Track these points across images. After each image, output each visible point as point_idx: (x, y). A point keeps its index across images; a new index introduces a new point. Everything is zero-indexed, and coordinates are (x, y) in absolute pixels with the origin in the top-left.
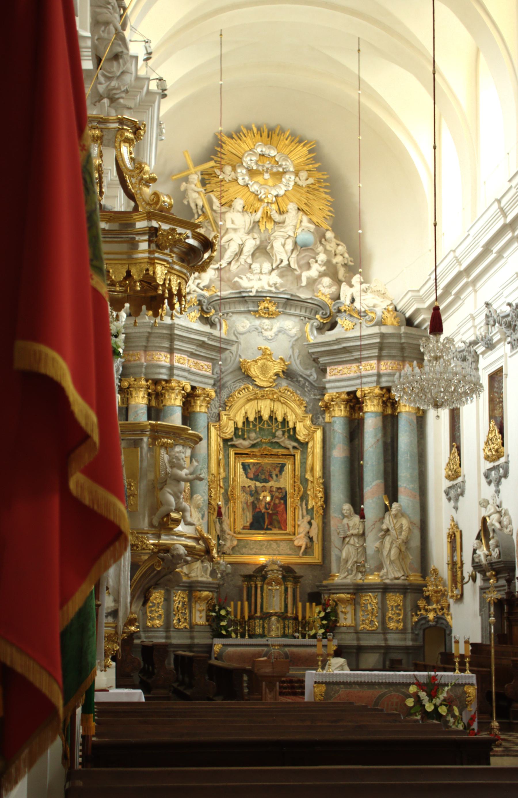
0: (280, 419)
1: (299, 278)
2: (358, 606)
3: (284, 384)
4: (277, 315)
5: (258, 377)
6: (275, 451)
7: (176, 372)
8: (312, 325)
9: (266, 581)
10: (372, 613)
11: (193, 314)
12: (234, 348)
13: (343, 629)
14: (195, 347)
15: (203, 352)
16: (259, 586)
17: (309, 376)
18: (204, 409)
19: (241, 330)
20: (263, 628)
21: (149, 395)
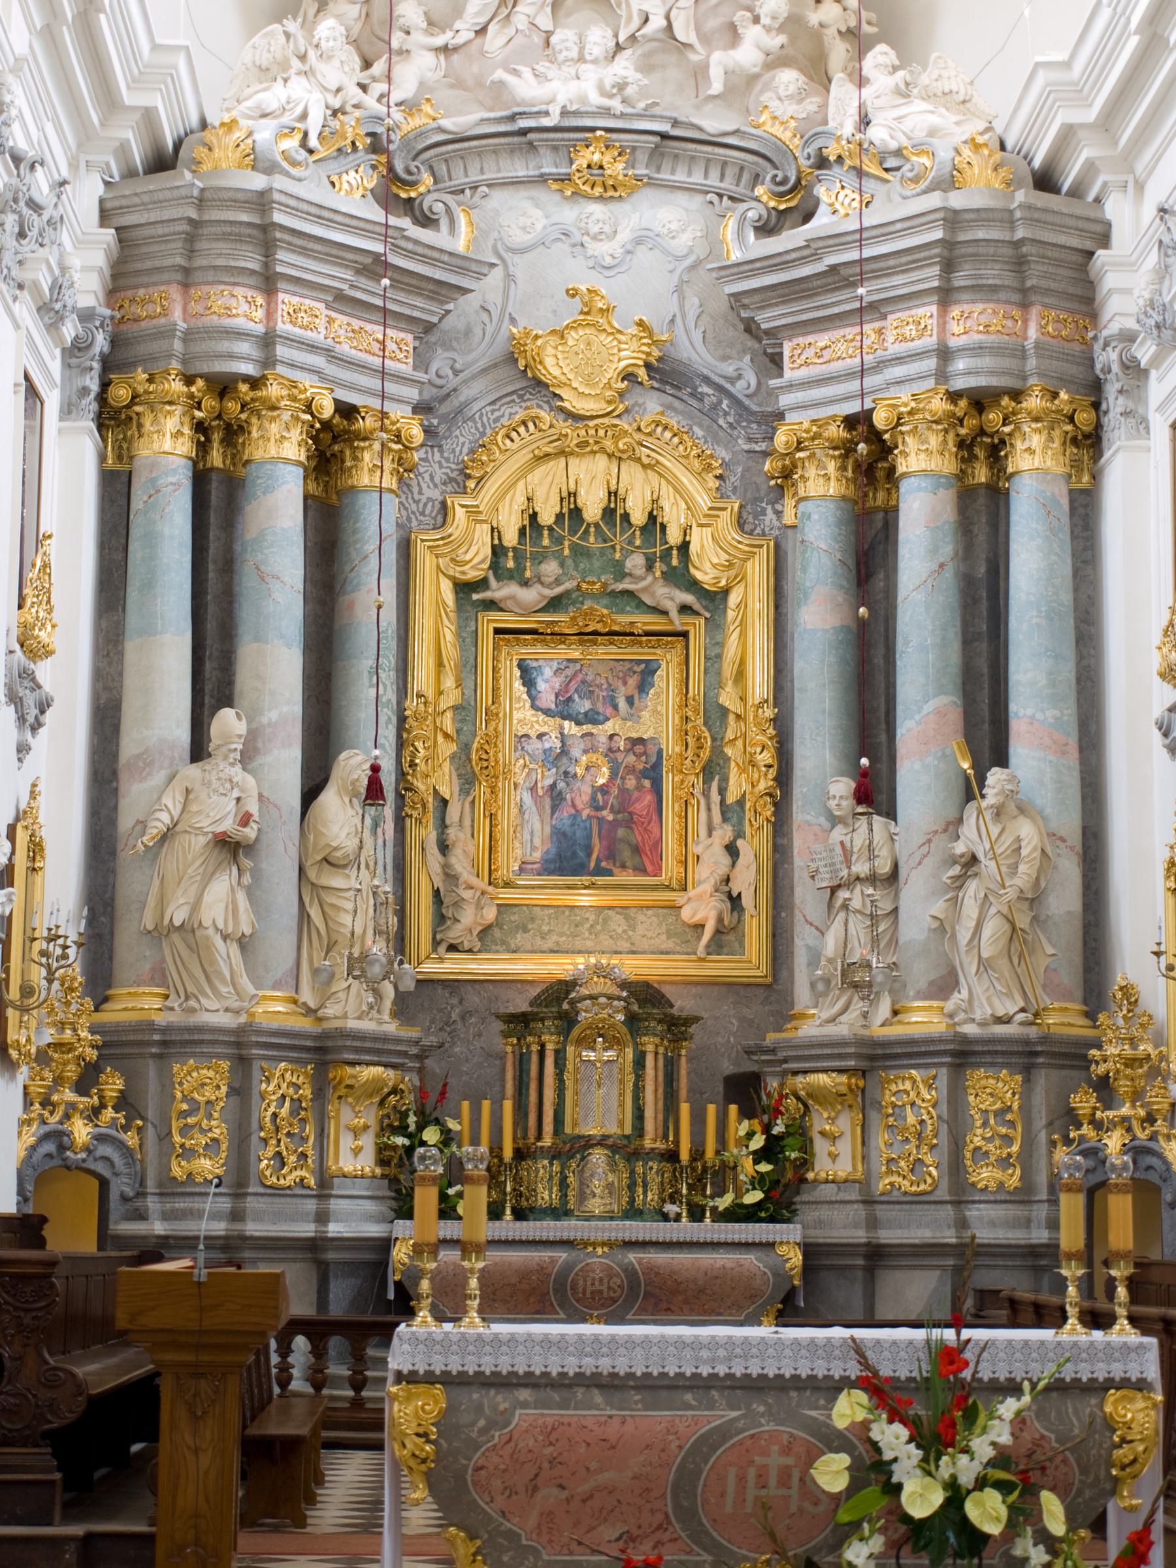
0: (638, 517)
1: (700, 73)
2: (873, 1115)
3: (652, 405)
4: (633, 190)
5: (567, 385)
6: (622, 620)
7: (281, 351)
8: (743, 218)
9: (575, 1032)
10: (919, 1136)
12: (489, 287)
13: (828, 1191)
14: (348, 275)
16: (550, 1047)
17: (732, 380)
19: (518, 238)
20: (564, 1185)
21: (200, 427)
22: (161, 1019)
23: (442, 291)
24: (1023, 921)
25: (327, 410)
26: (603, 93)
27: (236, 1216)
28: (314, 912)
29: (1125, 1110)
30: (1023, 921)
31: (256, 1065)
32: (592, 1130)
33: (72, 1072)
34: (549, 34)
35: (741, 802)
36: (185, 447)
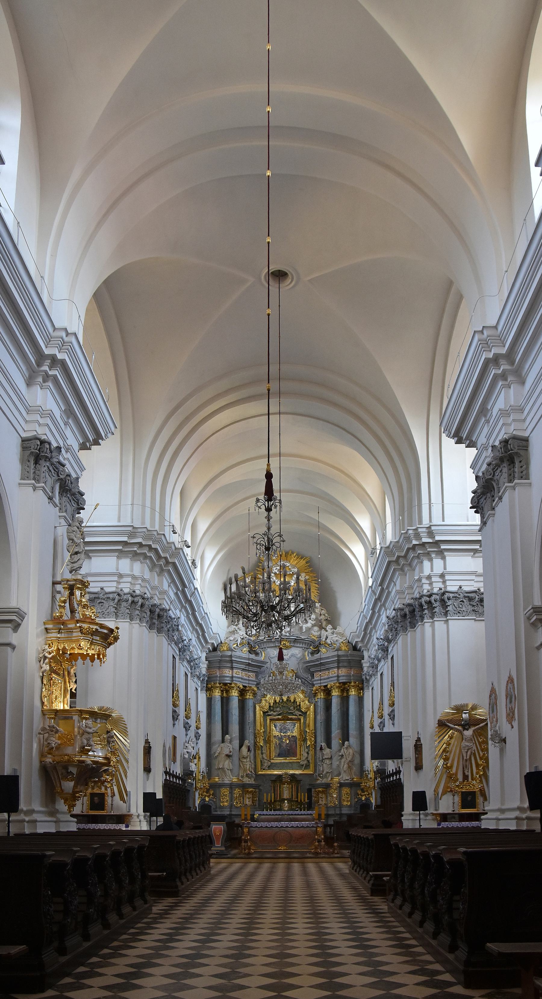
7: (234, 679)
11: (245, 649)
18: (251, 697)
21: (222, 691)
25: (241, 687)
29: (365, 793)
30: (350, 765)
32: (285, 797)
35: (309, 746)
36: (220, 694)
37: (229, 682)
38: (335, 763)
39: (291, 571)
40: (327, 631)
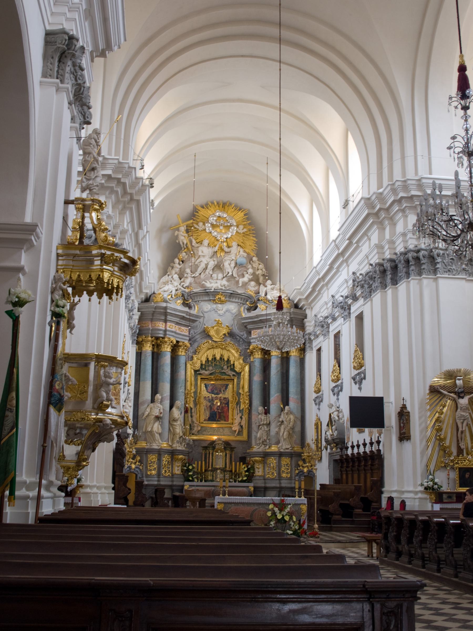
1: (238, 282)
2: (265, 465)
4: (226, 302)
8: (244, 308)
9: (215, 450)
10: (273, 468)
11: (179, 301)
12: (201, 320)
13: (258, 478)
14: (179, 319)
15: (183, 322)
16: (211, 452)
18: (183, 354)
20: (213, 476)
21: (153, 345)
22: (147, 447)
23: (194, 321)
24: (291, 432)
25: (175, 342)
26: (221, 286)
27: (158, 481)
28: (171, 429)
29: (307, 464)
30: (291, 432)
31: (162, 455)
33: (132, 456)
34: (212, 275)
37: (162, 336)
38: (274, 429)
39: (229, 222)
40: (266, 286)
